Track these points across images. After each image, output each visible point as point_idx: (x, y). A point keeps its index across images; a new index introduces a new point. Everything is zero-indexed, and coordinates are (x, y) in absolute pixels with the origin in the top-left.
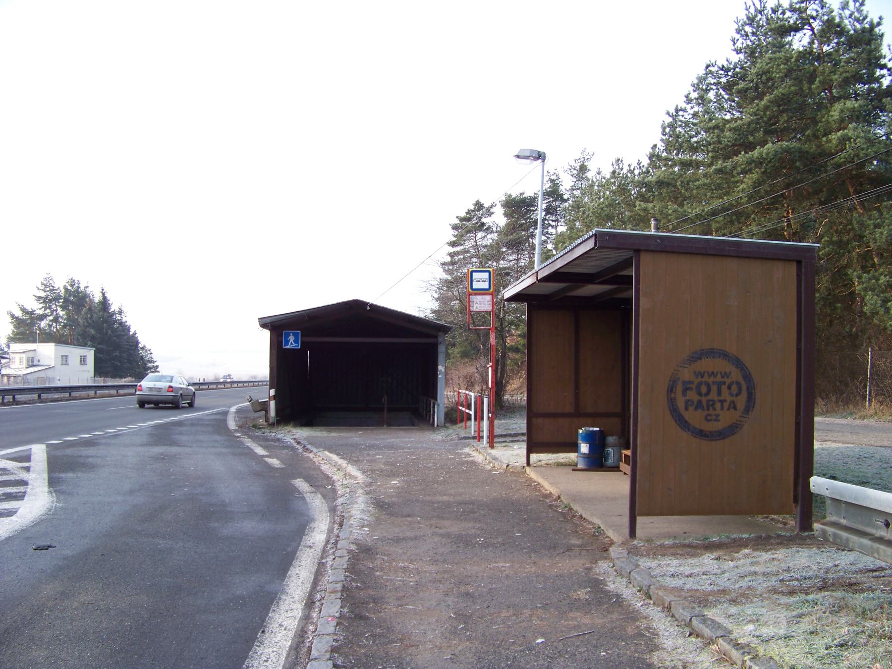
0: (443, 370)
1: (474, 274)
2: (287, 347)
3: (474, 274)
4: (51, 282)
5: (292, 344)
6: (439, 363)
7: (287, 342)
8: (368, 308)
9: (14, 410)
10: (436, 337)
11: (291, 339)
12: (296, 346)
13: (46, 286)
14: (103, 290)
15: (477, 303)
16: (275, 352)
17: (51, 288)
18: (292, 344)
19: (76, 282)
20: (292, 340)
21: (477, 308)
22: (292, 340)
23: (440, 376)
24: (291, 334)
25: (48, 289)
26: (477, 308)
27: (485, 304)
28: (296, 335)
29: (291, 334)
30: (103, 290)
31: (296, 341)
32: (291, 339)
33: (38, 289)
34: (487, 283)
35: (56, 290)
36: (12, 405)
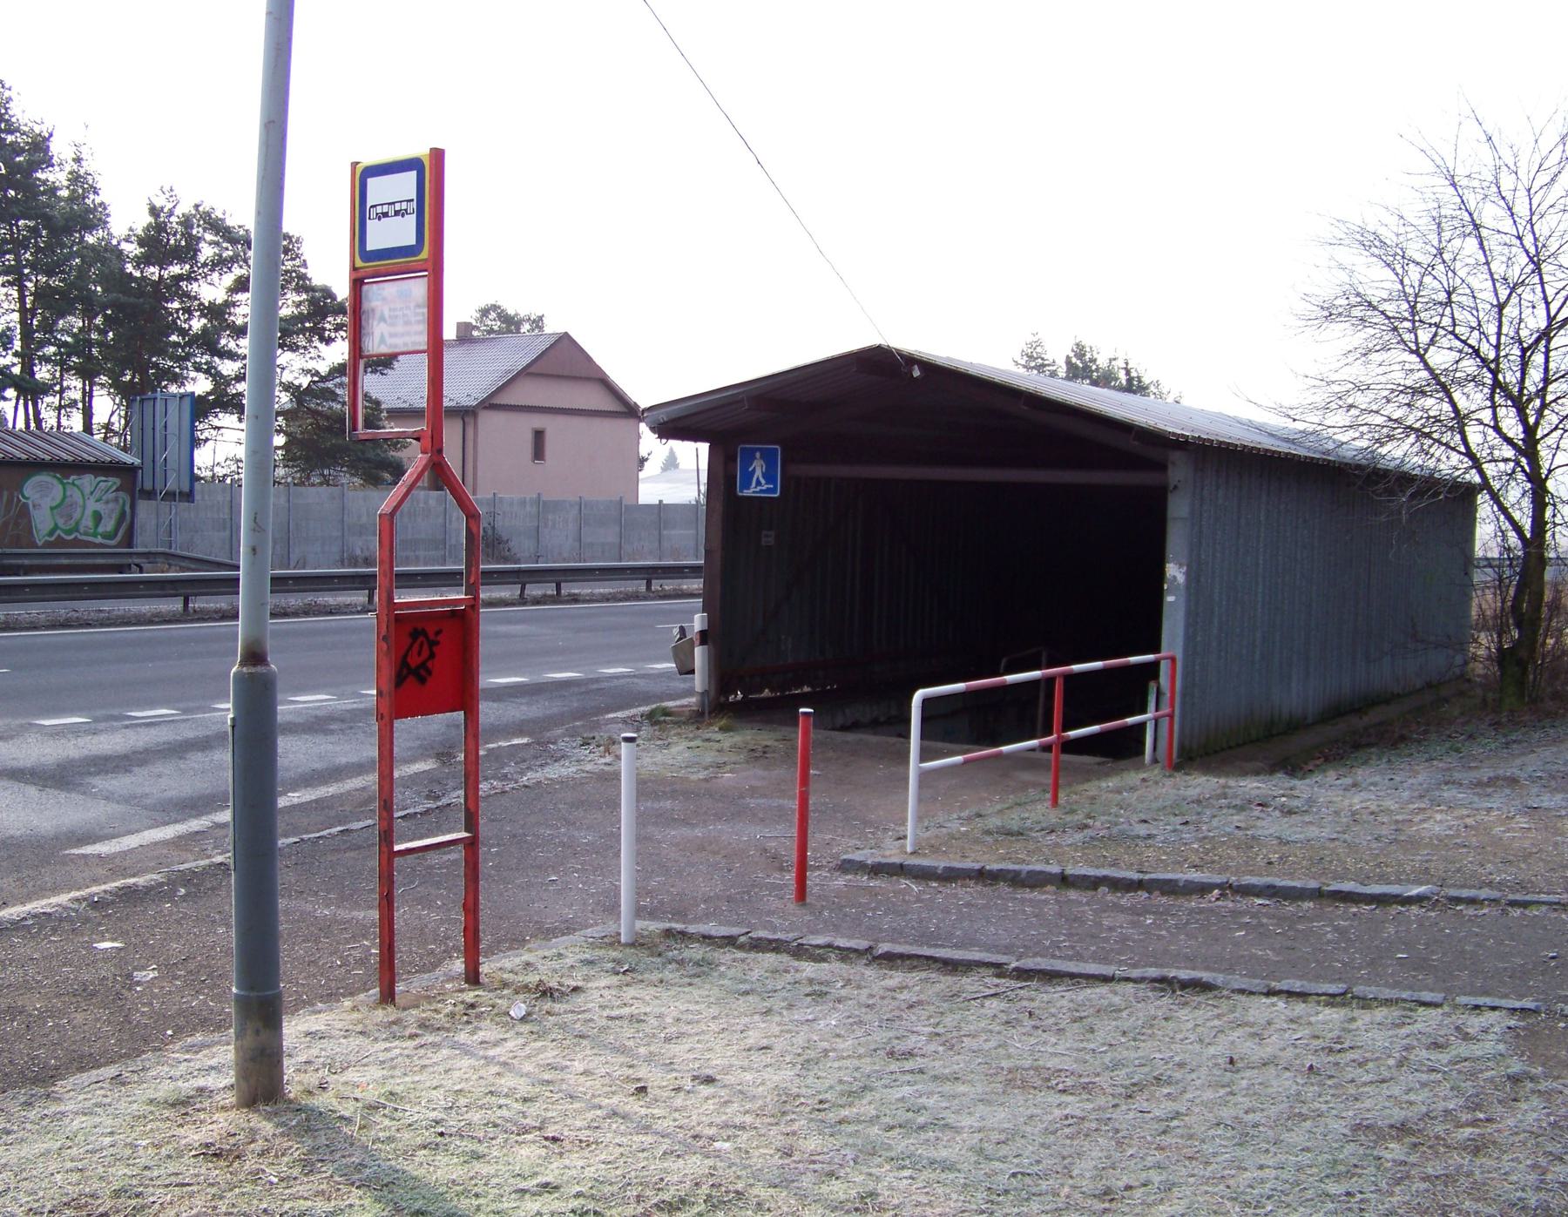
0: (1181, 578)
1: (371, 182)
2: (747, 493)
3: (371, 182)
4: (1039, 349)
5: (758, 483)
6: (1170, 555)
7: (748, 477)
8: (916, 373)
9: (674, 606)
10: (1162, 467)
11: (758, 468)
12: (768, 490)
13: (1031, 357)
14: (1127, 363)
15: (382, 319)
16: (719, 507)
17: (1040, 361)
18: (758, 483)
19: (1088, 349)
20: (758, 473)
21: (382, 340)
22: (758, 473)
23: (1170, 599)
24: (758, 455)
25: (1033, 364)
26: (382, 340)
27: (407, 323)
28: (769, 458)
29: (758, 455)
30: (1127, 363)
31: (769, 477)
32: (758, 468)
33: (1017, 364)
34: (411, 220)
35: (1049, 365)
36: (645, 599)
